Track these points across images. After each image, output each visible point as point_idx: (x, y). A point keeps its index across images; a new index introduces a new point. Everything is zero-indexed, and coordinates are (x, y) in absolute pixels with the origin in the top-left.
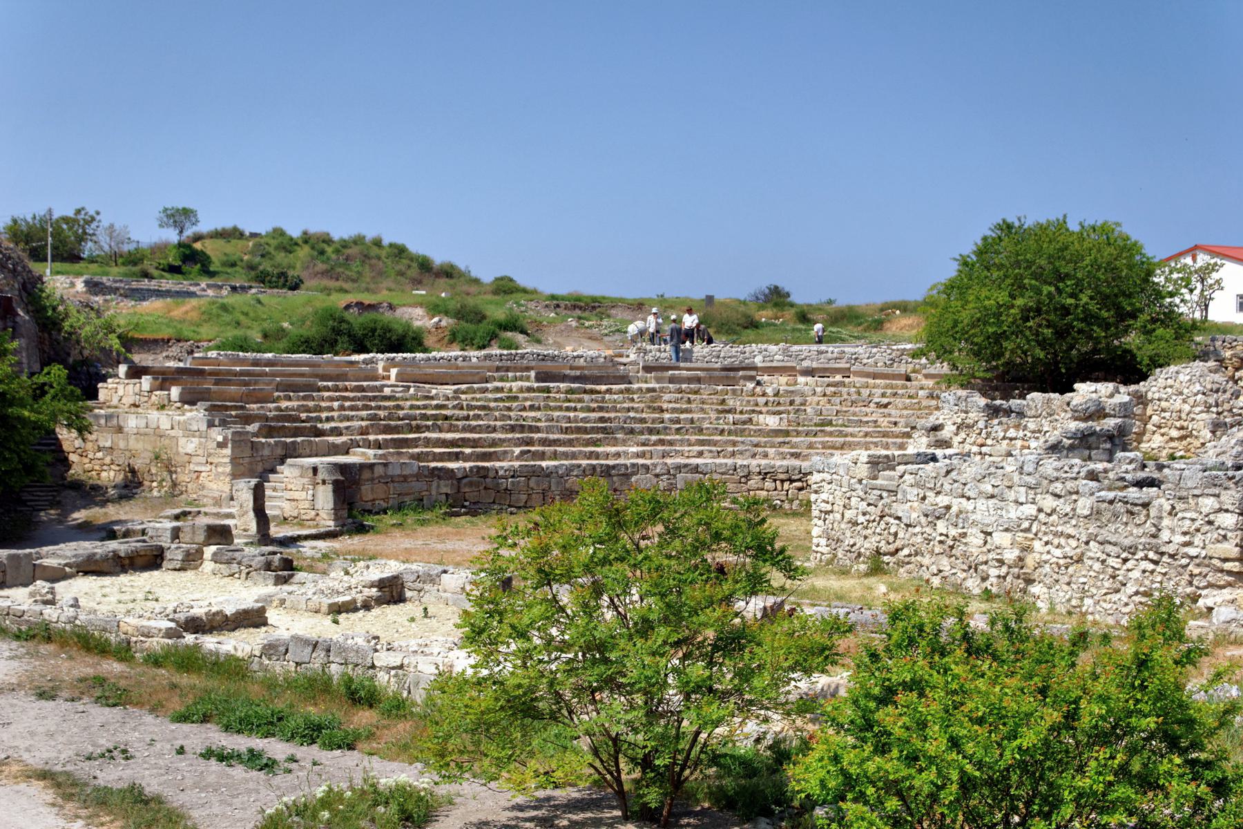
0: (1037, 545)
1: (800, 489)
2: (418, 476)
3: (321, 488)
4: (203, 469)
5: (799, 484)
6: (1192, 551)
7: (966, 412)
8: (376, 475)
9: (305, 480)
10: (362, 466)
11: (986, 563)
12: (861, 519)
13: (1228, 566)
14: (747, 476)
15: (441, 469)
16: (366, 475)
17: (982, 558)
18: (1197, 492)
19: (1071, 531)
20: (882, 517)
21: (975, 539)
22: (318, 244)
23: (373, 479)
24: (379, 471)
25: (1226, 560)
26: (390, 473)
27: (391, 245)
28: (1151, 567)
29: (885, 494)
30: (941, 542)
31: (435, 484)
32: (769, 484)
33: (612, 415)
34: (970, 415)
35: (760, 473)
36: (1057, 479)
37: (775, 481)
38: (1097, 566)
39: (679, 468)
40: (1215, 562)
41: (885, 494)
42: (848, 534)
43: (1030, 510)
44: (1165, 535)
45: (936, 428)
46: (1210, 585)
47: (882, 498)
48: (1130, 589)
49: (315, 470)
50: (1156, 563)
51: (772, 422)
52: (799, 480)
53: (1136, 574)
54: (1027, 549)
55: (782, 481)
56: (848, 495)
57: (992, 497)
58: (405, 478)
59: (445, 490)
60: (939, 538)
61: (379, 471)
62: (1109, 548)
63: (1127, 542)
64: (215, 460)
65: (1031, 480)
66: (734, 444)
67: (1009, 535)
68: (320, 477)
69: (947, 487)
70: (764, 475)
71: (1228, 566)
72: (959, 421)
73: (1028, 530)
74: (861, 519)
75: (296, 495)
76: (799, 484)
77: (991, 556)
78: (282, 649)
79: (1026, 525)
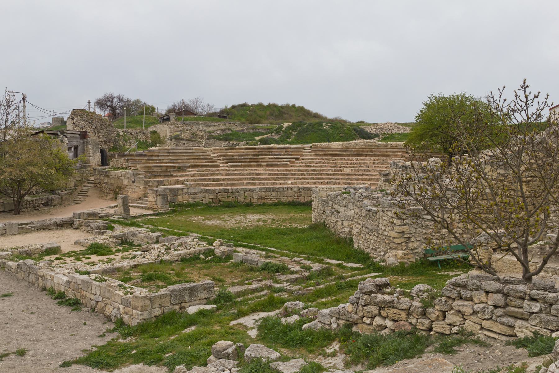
0: (354, 226)
2: (200, 192)
3: (158, 197)
6: (386, 233)
9: (154, 195)
10: (178, 189)
11: (342, 232)
12: (320, 212)
13: (395, 240)
15: (209, 190)
16: (180, 192)
17: (340, 231)
18: (387, 209)
19: (359, 221)
21: (340, 224)
22: (272, 107)
23: (183, 194)
24: (185, 190)
25: (394, 238)
27: (299, 107)
28: (376, 239)
31: (207, 195)
36: (359, 200)
38: (364, 237)
39: (304, 188)
40: (391, 238)
43: (352, 212)
44: (380, 225)
45: (387, 175)
46: (391, 248)
48: (371, 248)
49: (157, 191)
50: (378, 237)
51: (348, 171)
53: (372, 241)
54: (351, 228)
57: (345, 206)
58: (196, 193)
59: (211, 197)
61: (185, 190)
62: (367, 230)
63: (370, 228)
65: (352, 200)
66: (330, 179)
67: (347, 222)
68: (158, 193)
71: (395, 240)
73: (352, 220)
75: (152, 200)
77: (343, 230)
79: (352, 218)
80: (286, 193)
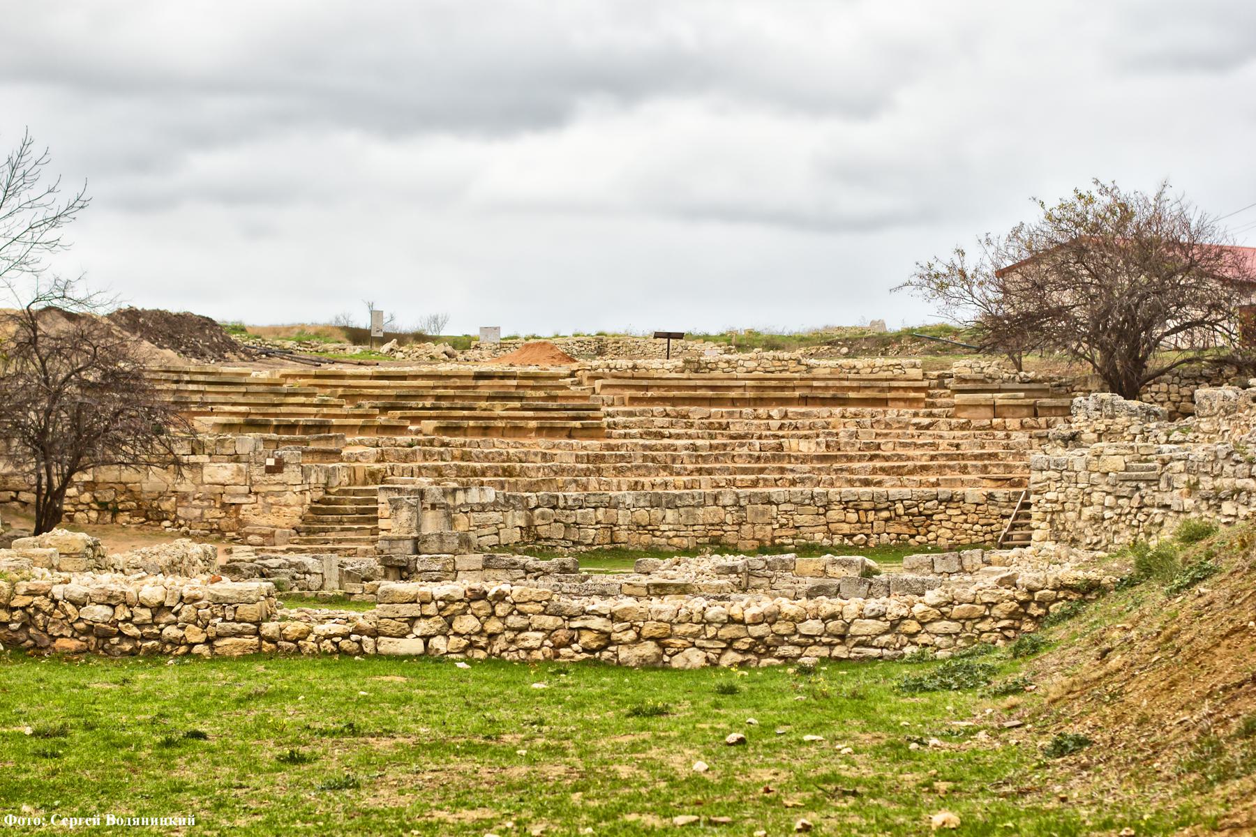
1: (887, 520)
4: (244, 500)
5: (885, 514)
7: (1113, 417)
8: (458, 503)
14: (827, 507)
20: (1139, 508)
26: (469, 501)
29: (1142, 485)
30: (1227, 523)
32: (852, 516)
33: (958, 399)
34: (1118, 420)
35: (840, 502)
37: (857, 511)
41: (1142, 485)
42: (1089, 531)
47: (1138, 489)
51: (806, 447)
52: (887, 509)
55: (866, 511)
56: (1088, 490)
60: (1224, 520)
64: (263, 489)
69: (1228, 469)
70: (846, 505)
72: (1103, 427)
74: (1108, 514)
76: (885, 514)
78: (834, 590)
80: (700, 511)
